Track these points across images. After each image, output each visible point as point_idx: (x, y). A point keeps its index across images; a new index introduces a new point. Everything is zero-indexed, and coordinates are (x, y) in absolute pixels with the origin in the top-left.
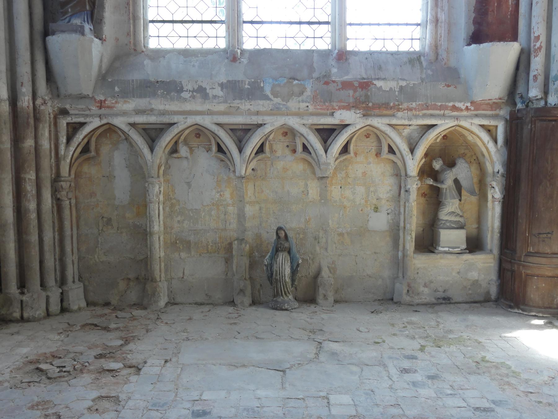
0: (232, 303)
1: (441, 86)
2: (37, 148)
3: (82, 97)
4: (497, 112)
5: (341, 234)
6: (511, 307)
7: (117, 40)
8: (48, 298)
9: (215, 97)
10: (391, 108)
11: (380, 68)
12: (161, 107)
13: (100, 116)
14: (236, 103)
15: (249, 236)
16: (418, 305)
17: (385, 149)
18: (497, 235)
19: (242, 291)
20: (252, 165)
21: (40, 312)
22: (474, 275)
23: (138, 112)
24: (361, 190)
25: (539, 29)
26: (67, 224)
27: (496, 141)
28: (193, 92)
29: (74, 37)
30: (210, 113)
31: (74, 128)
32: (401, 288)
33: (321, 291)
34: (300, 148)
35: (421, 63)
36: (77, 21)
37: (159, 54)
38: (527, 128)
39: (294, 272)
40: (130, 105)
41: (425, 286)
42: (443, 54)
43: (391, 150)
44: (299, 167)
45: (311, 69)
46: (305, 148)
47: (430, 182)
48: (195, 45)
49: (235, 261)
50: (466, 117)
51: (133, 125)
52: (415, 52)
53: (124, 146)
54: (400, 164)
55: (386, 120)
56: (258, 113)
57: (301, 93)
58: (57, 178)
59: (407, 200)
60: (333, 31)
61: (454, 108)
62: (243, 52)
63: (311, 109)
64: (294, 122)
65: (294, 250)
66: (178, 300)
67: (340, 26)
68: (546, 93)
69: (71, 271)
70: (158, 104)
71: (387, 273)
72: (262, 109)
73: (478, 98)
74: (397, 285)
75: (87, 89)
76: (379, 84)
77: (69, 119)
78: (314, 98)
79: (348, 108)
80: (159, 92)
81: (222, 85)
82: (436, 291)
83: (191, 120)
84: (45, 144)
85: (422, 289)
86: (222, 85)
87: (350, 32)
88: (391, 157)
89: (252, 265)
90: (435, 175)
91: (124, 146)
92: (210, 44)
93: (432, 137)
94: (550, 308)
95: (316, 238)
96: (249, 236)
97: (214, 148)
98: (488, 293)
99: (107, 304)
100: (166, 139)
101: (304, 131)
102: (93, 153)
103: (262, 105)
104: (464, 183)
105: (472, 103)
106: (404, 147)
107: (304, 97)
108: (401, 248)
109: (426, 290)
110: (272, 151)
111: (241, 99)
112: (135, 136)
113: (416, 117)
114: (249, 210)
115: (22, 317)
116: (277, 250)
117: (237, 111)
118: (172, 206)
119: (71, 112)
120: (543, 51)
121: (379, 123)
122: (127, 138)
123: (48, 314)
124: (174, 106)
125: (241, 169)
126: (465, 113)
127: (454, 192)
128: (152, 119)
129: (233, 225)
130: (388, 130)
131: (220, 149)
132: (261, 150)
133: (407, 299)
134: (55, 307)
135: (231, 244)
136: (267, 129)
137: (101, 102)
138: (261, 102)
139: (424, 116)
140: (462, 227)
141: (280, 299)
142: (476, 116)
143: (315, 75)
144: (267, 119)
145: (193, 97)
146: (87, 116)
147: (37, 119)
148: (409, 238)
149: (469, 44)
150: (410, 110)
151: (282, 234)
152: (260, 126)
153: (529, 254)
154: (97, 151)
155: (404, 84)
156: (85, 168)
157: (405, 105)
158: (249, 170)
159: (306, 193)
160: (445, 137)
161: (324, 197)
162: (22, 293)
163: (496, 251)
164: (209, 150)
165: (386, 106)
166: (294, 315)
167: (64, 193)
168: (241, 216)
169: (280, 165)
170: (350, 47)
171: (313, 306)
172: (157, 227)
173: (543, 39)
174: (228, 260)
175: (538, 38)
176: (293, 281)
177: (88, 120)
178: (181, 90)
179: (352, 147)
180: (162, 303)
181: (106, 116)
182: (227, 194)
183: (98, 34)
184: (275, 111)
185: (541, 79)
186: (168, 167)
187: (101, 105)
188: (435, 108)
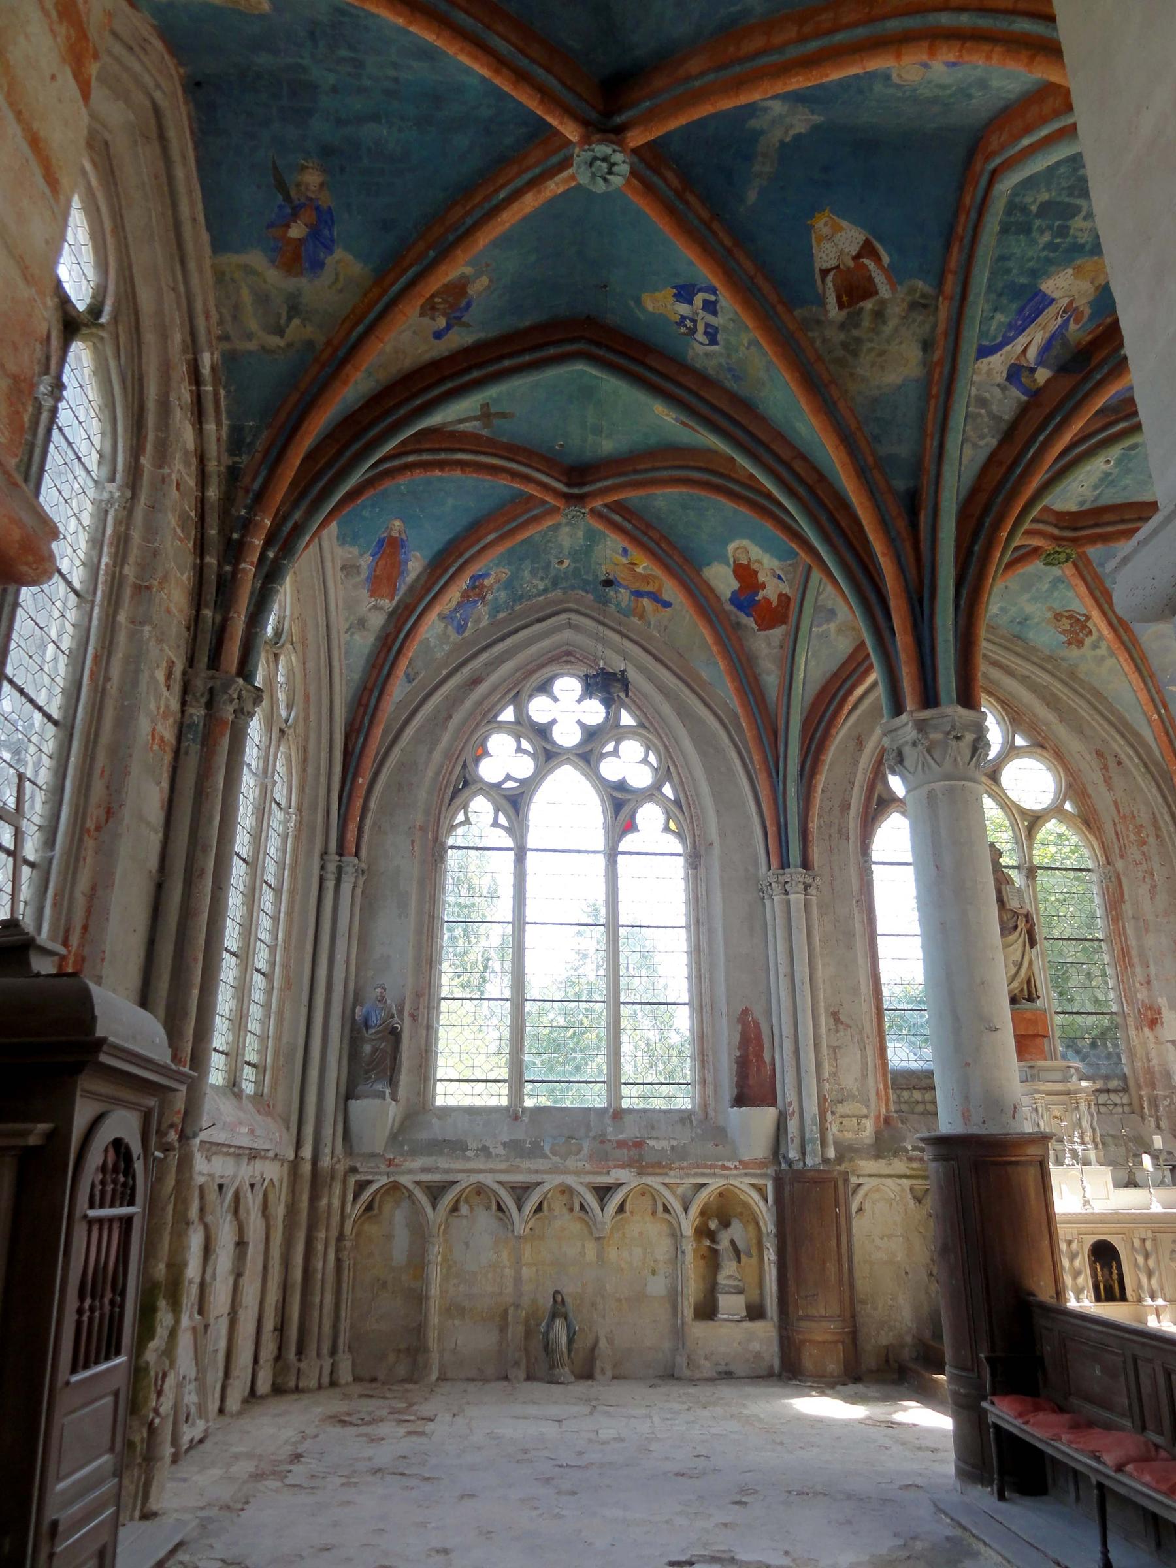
0: (506, 1378)
1: (710, 1145)
2: (329, 1205)
3: (373, 1156)
4: (765, 1171)
5: (619, 1300)
6: (790, 1379)
7: (408, 1099)
8: (321, 1368)
9: (497, 1156)
10: (664, 1167)
11: (653, 1127)
12: (446, 1166)
13: (388, 1174)
14: (517, 1162)
15: (526, 1301)
16: (699, 1380)
17: (660, 1208)
18: (775, 1301)
19: (517, 1364)
20: (530, 1225)
21: (313, 1383)
22: (756, 1346)
23: (424, 1170)
24: (638, 1251)
25: (791, 1096)
26: (345, 1286)
27: (766, 1200)
28: (478, 1149)
29: (377, 1101)
30: (492, 1171)
31: (362, 1186)
32: (681, 1360)
33: (598, 1364)
34: (577, 1207)
35: (691, 1122)
36: (379, 1087)
37: (447, 1111)
38: (788, 1188)
39: (570, 1341)
40: (418, 1163)
41: (706, 1358)
42: (711, 1113)
43: (666, 1210)
44: (576, 1227)
45: (588, 1128)
46: (582, 1207)
47: (707, 1243)
48: (479, 1102)
49: (510, 1330)
50: (736, 1176)
51: (418, 1183)
52: (686, 1110)
53: (406, 1204)
54: (674, 1223)
55: (660, 1179)
56: (537, 1172)
57: (579, 1151)
58: (341, 1237)
59: (683, 1262)
60: (609, 1090)
61: (724, 1167)
62: (525, 1109)
63: (588, 1167)
64: (571, 1181)
65: (571, 1315)
66: (449, 1375)
67: (615, 1086)
68: (803, 1154)
69: (342, 1341)
70: (443, 1163)
71: (667, 1345)
72: (542, 1168)
73: (745, 1158)
74: (678, 1358)
75: (379, 1150)
76: (651, 1143)
77: (358, 1177)
78: (591, 1157)
79: (623, 1167)
80: (446, 1151)
81: (504, 1144)
82: (718, 1364)
83: (474, 1178)
84: (336, 1203)
85: (702, 1362)
86: (504, 1144)
87: (625, 1090)
88: (666, 1216)
89: (528, 1334)
90: (712, 1236)
91: (406, 1204)
92: (493, 1102)
93: (704, 1195)
94: (824, 1376)
95: (593, 1304)
96: (526, 1301)
97: (494, 1207)
98: (772, 1367)
99: (373, 1380)
101: (581, 1189)
102: (376, 1211)
103: (540, 1164)
104: (741, 1245)
105: (740, 1162)
106: (677, 1206)
107: (580, 1156)
108: (680, 1315)
109: (707, 1364)
110: (551, 1210)
111: (521, 1157)
112: (419, 1194)
113: (688, 1175)
114: (526, 1272)
115: (297, 1387)
116: (554, 1315)
117: (517, 1170)
118: (450, 1267)
119: (361, 1170)
120: (797, 1114)
121: (651, 1181)
122: (411, 1195)
123: (320, 1387)
124: (458, 1165)
125: (520, 1229)
126: (735, 1172)
127: (732, 1254)
128: (437, 1177)
129: (510, 1289)
130: (662, 1189)
131: (500, 1208)
132: (539, 1209)
133: (687, 1373)
134: (326, 1380)
135: (505, 1314)
136: (546, 1187)
137: (390, 1160)
138: (541, 1161)
139: (696, 1175)
140: (741, 1292)
141: (556, 1371)
142: (746, 1175)
143: (592, 1134)
144: (546, 1177)
145: (477, 1156)
146: (376, 1174)
147: (332, 1178)
148: (686, 1303)
149: (733, 1106)
150: (682, 1168)
151: (559, 1299)
152: (540, 1184)
153: (800, 1319)
154: (380, 1207)
155: (674, 1143)
156: (367, 1227)
157: (677, 1165)
158: (528, 1229)
159: (583, 1254)
160: (721, 1194)
162: (299, 1360)
163: (776, 1319)
164: (488, 1208)
165: (659, 1165)
166: (570, 1387)
167: (346, 1253)
168: (518, 1280)
169: (558, 1224)
170: (625, 1104)
171: (590, 1382)
172: (434, 1291)
173: (795, 1105)
174: (503, 1329)
175: (790, 1103)
176: (570, 1350)
177: (376, 1178)
178: (467, 1149)
179: (627, 1207)
180: (434, 1376)
181: (393, 1173)
182: (505, 1255)
183: (394, 1098)
184: (555, 1170)
185: (797, 1141)
186: (448, 1226)
187: (390, 1163)
188: (706, 1167)
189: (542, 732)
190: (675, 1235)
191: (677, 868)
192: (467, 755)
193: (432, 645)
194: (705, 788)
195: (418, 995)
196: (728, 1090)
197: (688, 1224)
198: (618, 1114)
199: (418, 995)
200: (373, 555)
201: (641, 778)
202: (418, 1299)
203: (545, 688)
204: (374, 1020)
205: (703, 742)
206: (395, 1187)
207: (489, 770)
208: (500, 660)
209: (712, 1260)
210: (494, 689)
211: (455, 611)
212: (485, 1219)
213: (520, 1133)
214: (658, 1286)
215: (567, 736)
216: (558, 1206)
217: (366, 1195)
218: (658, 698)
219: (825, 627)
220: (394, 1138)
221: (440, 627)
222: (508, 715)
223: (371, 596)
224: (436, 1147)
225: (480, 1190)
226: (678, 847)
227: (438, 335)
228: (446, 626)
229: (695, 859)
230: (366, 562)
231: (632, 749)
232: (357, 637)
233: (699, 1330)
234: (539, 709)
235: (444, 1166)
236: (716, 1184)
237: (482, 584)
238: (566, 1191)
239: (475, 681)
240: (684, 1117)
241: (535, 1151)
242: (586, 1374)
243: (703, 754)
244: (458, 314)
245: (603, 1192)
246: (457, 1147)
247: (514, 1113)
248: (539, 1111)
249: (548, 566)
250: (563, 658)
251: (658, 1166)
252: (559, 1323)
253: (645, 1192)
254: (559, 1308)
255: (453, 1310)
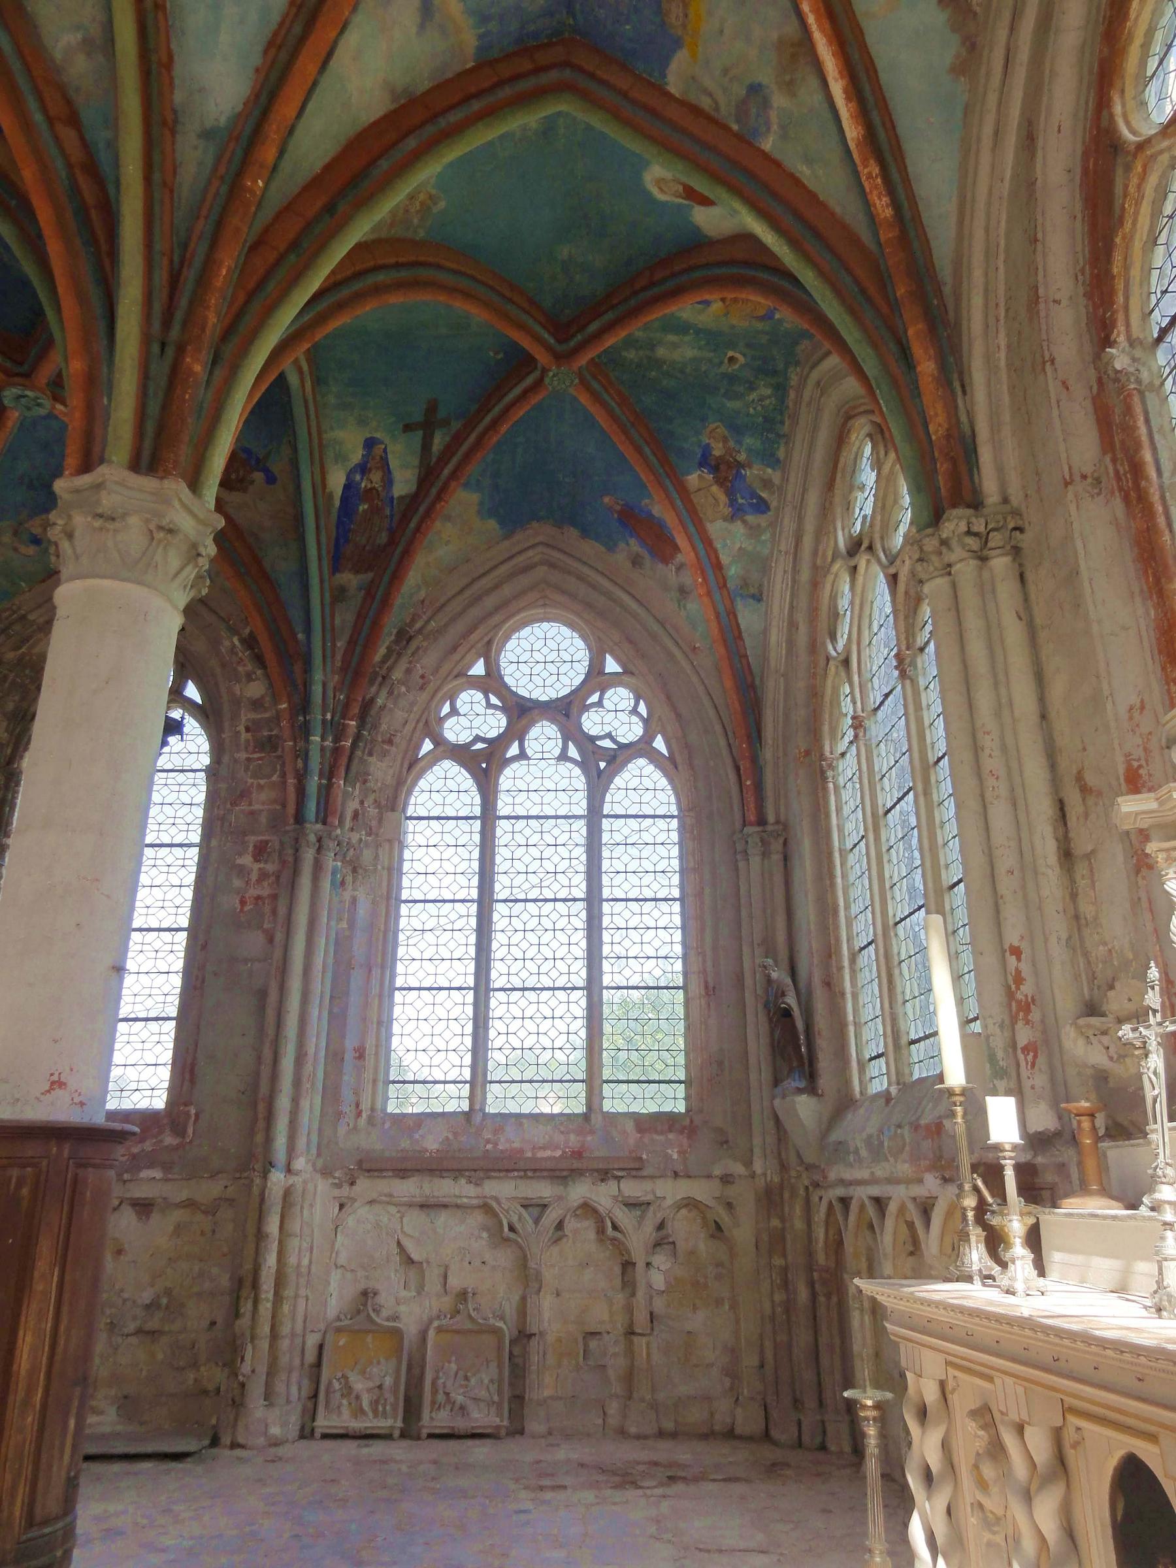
193: (750, 548)
200: (632, 536)
211: (732, 502)
219: (773, 116)
221: (738, 528)
223: (667, 565)
227: (271, 479)
228: (744, 522)
230: (635, 546)
232: (689, 606)
237: (717, 458)
244: (253, 462)
249: (732, 379)
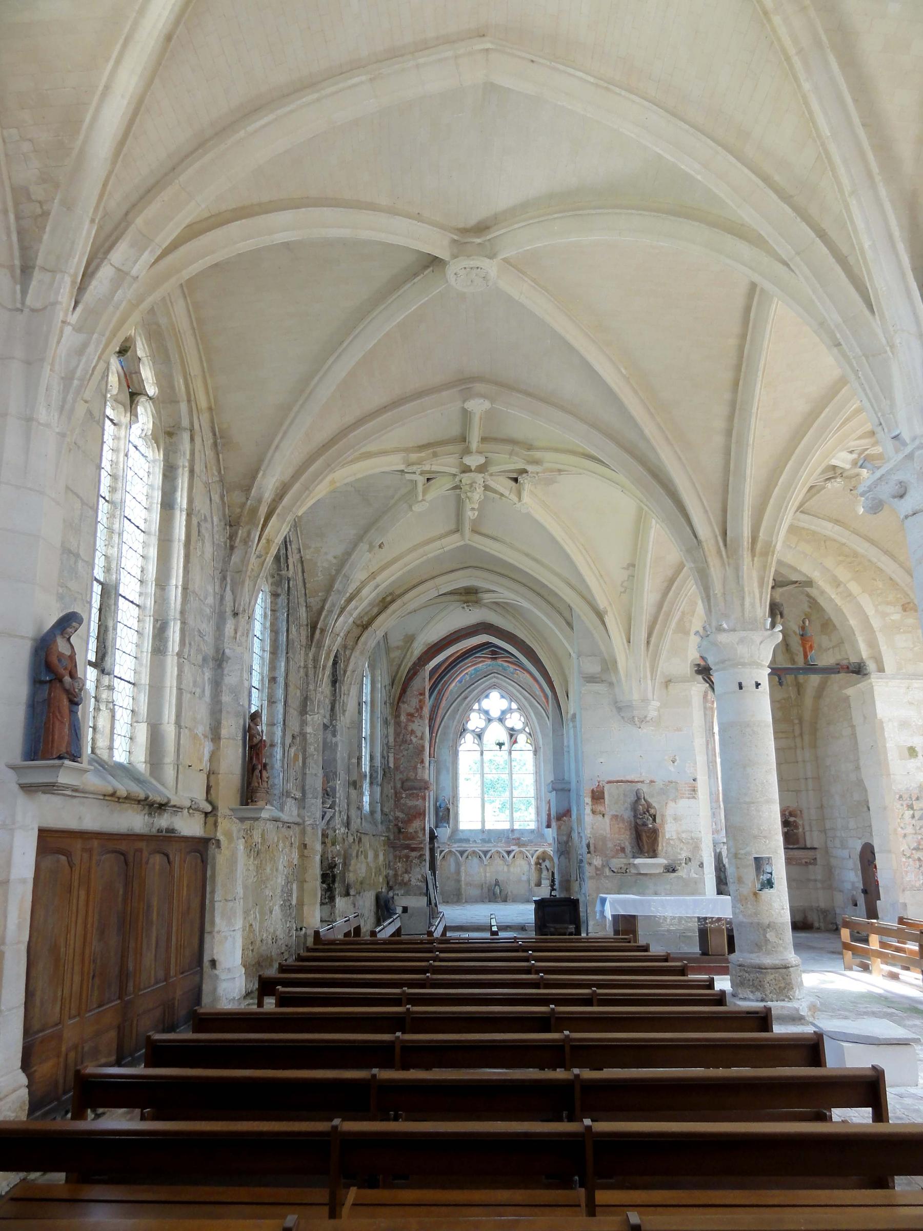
23: (458, 847)
31: (441, 852)
36: (445, 825)
37: (463, 831)
39: (500, 892)
40: (456, 845)
44: (501, 862)
64: (500, 849)
70: (464, 845)
89: (489, 890)
90: (540, 864)
100: (465, 854)
103: (490, 845)
106: (530, 857)
114: (488, 875)
116: (495, 886)
117: (485, 847)
121: (522, 849)
135: (482, 885)
161: (509, 871)
168: (485, 877)
172: (463, 879)
174: (482, 889)
184: (494, 846)
189: (487, 712)
190: (529, 864)
191: (530, 755)
192: (464, 721)
194: (538, 728)
195: (454, 797)
196: (545, 824)
197: (533, 861)
198: (513, 831)
199: (454, 797)
201: (519, 725)
202: (458, 881)
203: (487, 696)
204: (443, 806)
205: (537, 714)
206: (450, 851)
207: (471, 726)
208: (473, 690)
209: (540, 871)
210: (472, 699)
212: (476, 860)
213: (485, 836)
214: (524, 878)
215: (495, 714)
216: (496, 856)
217: (443, 854)
218: (523, 700)
220: (449, 838)
222: (476, 706)
224: (461, 841)
225: (474, 852)
226: (531, 748)
229: (536, 752)
231: (516, 715)
233: (536, 889)
234: (486, 704)
235: (465, 846)
236: (541, 850)
238: (498, 852)
239: (466, 698)
240: (532, 831)
241: (489, 841)
242: (505, 900)
243: (538, 719)
245: (509, 853)
246: (467, 841)
247: (483, 831)
248: (490, 831)
250: (494, 686)
251: (524, 845)
252: (497, 887)
253: (521, 852)
254: (497, 883)
255: (468, 884)
